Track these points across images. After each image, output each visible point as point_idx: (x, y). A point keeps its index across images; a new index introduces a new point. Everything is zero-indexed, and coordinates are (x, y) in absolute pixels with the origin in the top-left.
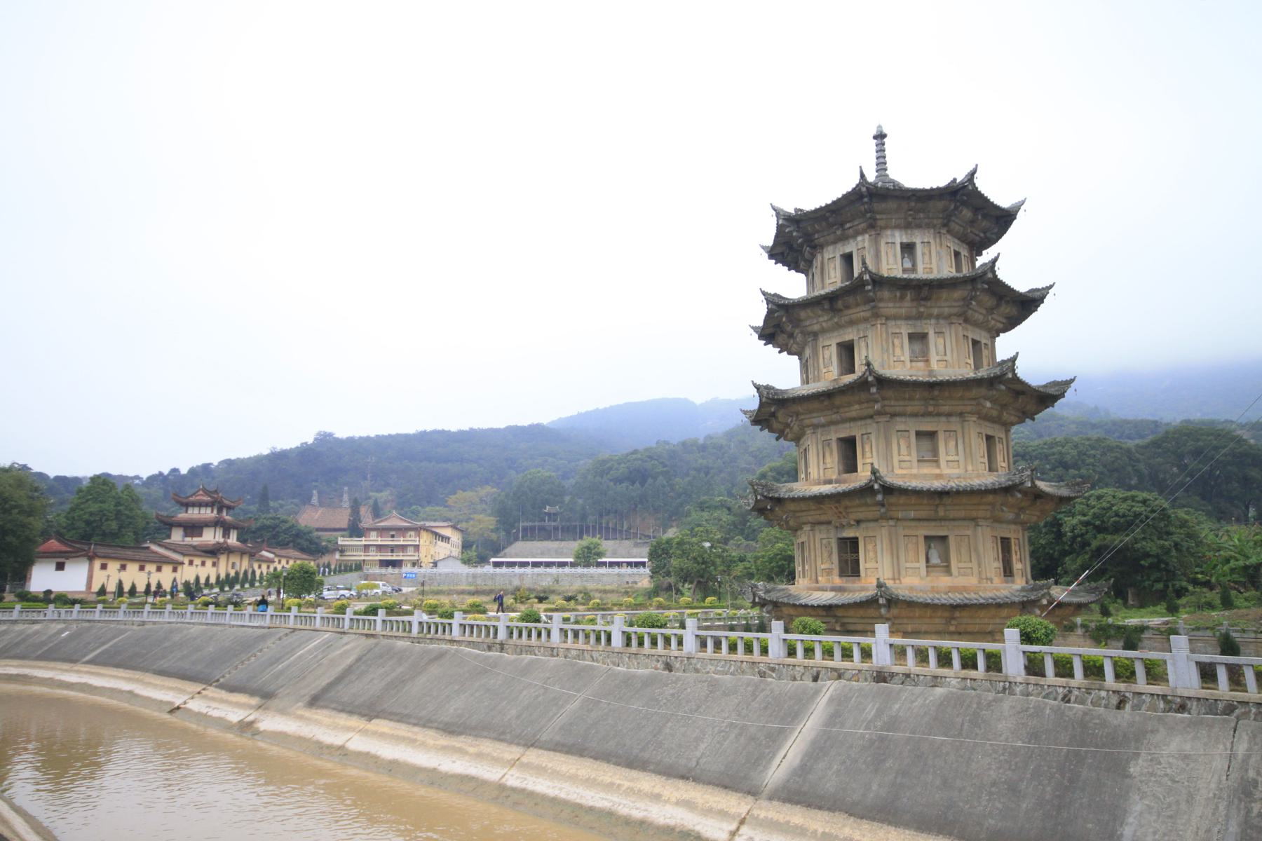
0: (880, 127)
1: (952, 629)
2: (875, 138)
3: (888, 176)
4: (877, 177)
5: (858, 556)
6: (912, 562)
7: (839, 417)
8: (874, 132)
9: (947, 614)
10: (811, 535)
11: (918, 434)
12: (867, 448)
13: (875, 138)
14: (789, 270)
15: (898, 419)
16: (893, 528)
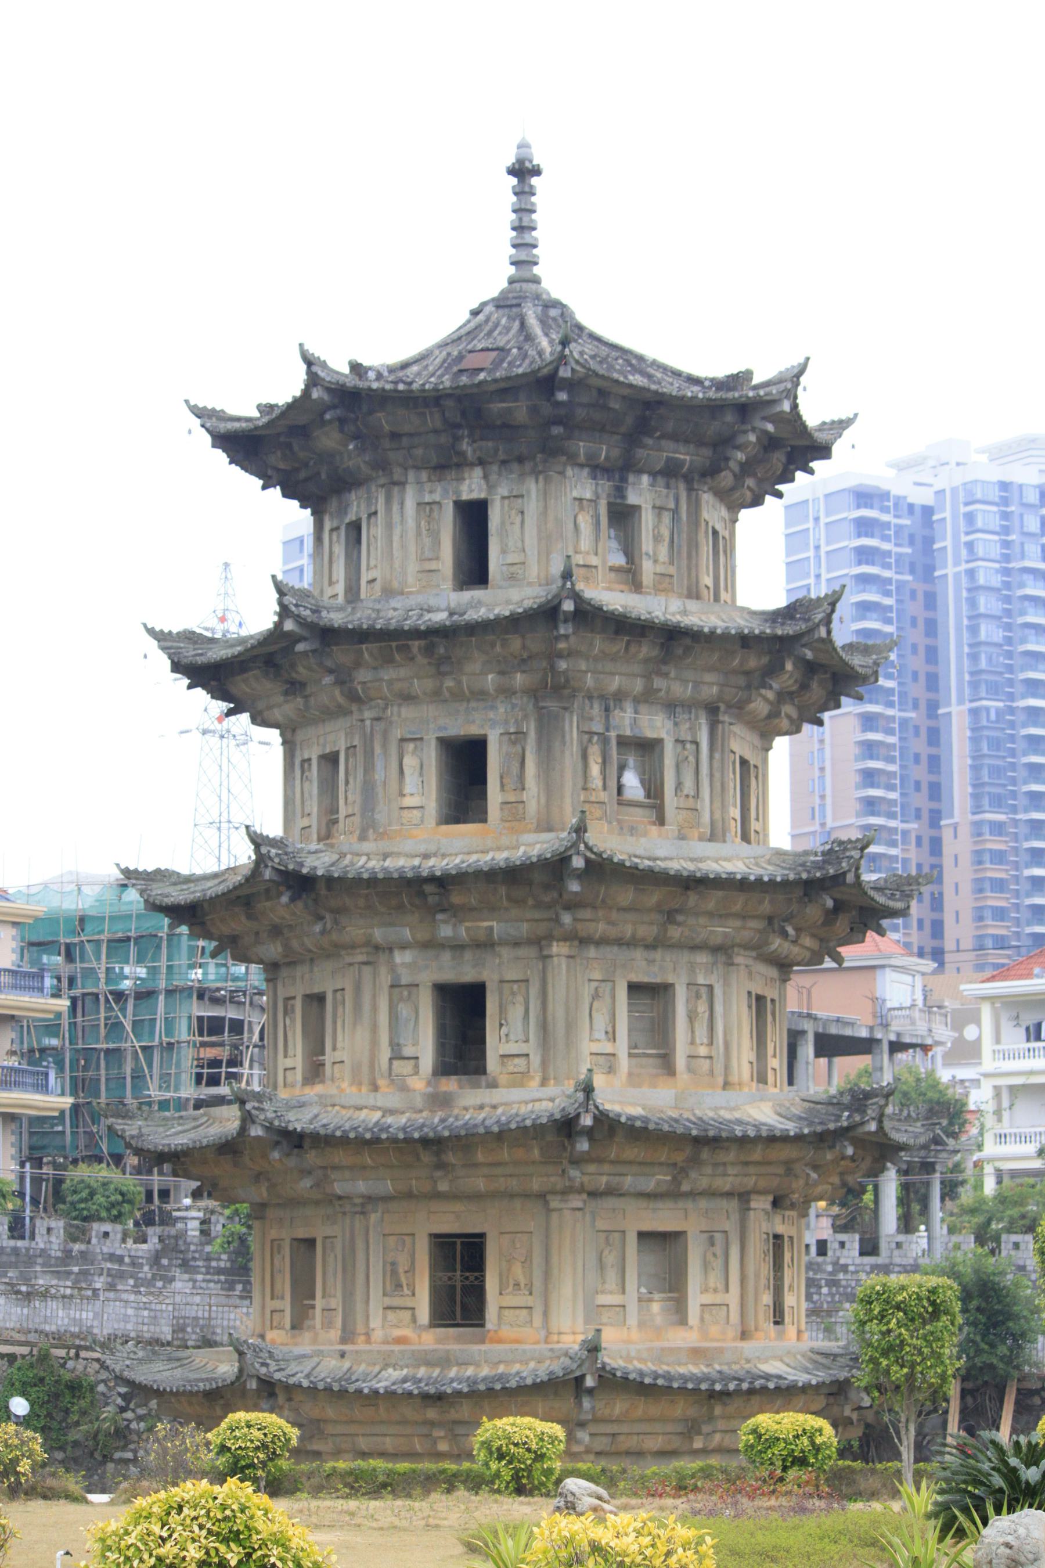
0: (523, 146)
1: (698, 1443)
2: (512, 172)
3: (536, 280)
4: (512, 281)
5: (482, 1280)
6: (611, 1293)
7: (463, 932)
8: (510, 160)
9: (692, 1412)
10: (357, 1224)
11: (634, 988)
12: (516, 1013)
13: (512, 172)
14: (231, 463)
15: (592, 952)
16: (579, 1214)
